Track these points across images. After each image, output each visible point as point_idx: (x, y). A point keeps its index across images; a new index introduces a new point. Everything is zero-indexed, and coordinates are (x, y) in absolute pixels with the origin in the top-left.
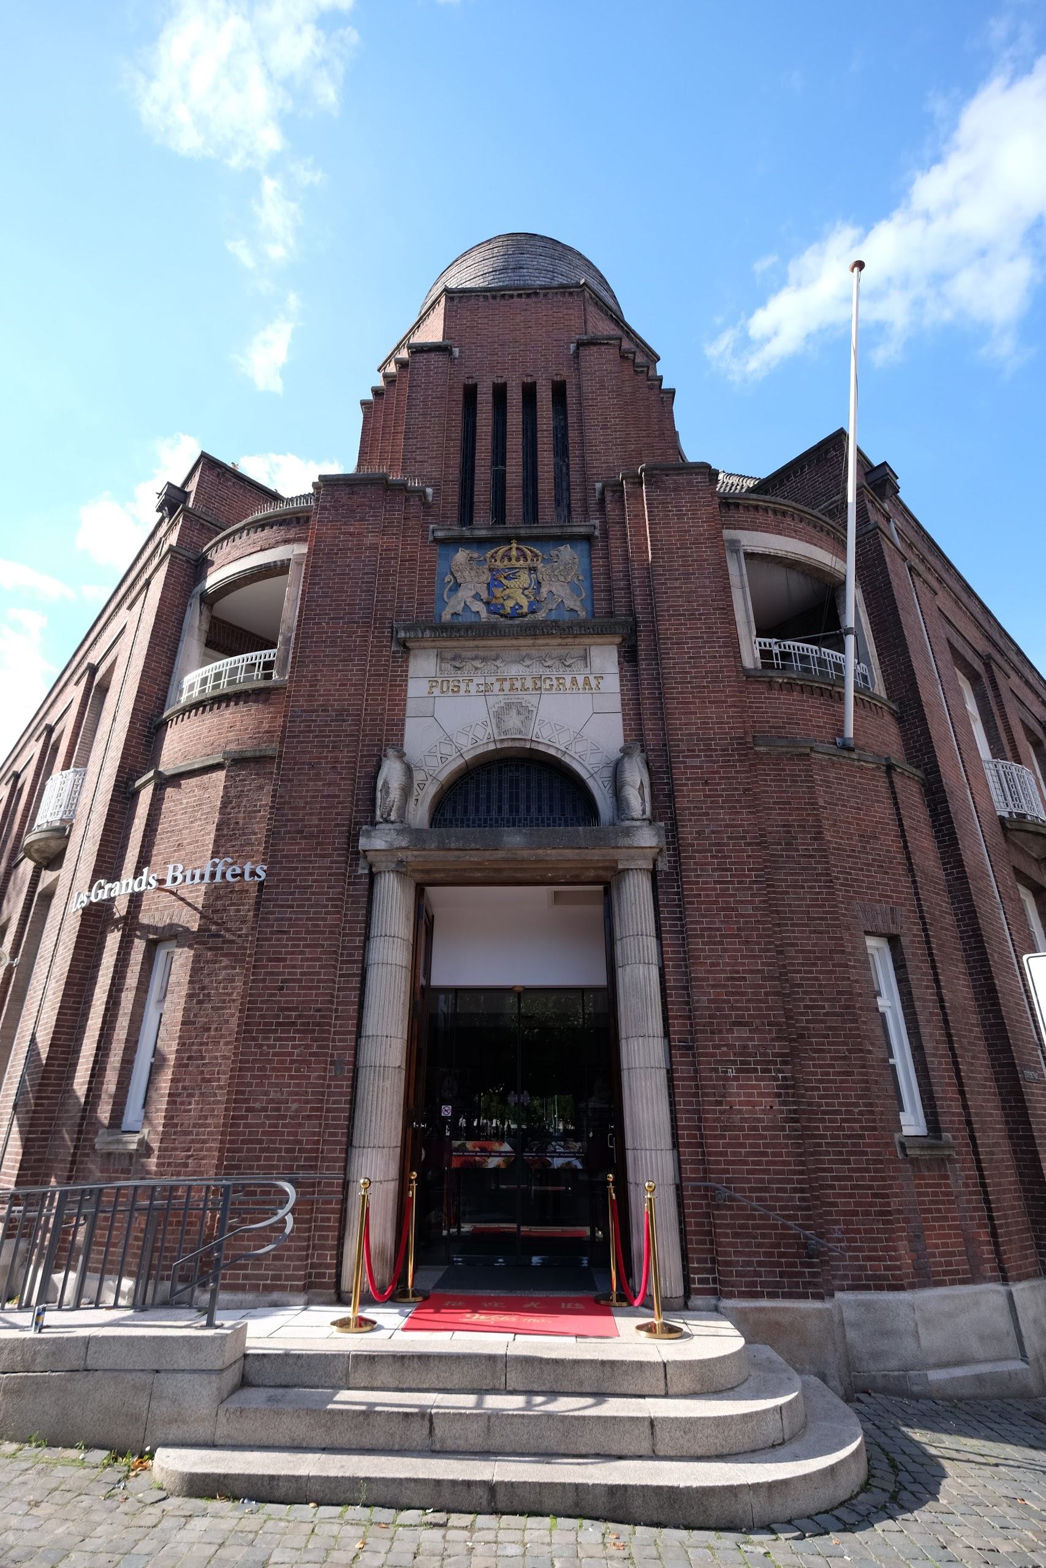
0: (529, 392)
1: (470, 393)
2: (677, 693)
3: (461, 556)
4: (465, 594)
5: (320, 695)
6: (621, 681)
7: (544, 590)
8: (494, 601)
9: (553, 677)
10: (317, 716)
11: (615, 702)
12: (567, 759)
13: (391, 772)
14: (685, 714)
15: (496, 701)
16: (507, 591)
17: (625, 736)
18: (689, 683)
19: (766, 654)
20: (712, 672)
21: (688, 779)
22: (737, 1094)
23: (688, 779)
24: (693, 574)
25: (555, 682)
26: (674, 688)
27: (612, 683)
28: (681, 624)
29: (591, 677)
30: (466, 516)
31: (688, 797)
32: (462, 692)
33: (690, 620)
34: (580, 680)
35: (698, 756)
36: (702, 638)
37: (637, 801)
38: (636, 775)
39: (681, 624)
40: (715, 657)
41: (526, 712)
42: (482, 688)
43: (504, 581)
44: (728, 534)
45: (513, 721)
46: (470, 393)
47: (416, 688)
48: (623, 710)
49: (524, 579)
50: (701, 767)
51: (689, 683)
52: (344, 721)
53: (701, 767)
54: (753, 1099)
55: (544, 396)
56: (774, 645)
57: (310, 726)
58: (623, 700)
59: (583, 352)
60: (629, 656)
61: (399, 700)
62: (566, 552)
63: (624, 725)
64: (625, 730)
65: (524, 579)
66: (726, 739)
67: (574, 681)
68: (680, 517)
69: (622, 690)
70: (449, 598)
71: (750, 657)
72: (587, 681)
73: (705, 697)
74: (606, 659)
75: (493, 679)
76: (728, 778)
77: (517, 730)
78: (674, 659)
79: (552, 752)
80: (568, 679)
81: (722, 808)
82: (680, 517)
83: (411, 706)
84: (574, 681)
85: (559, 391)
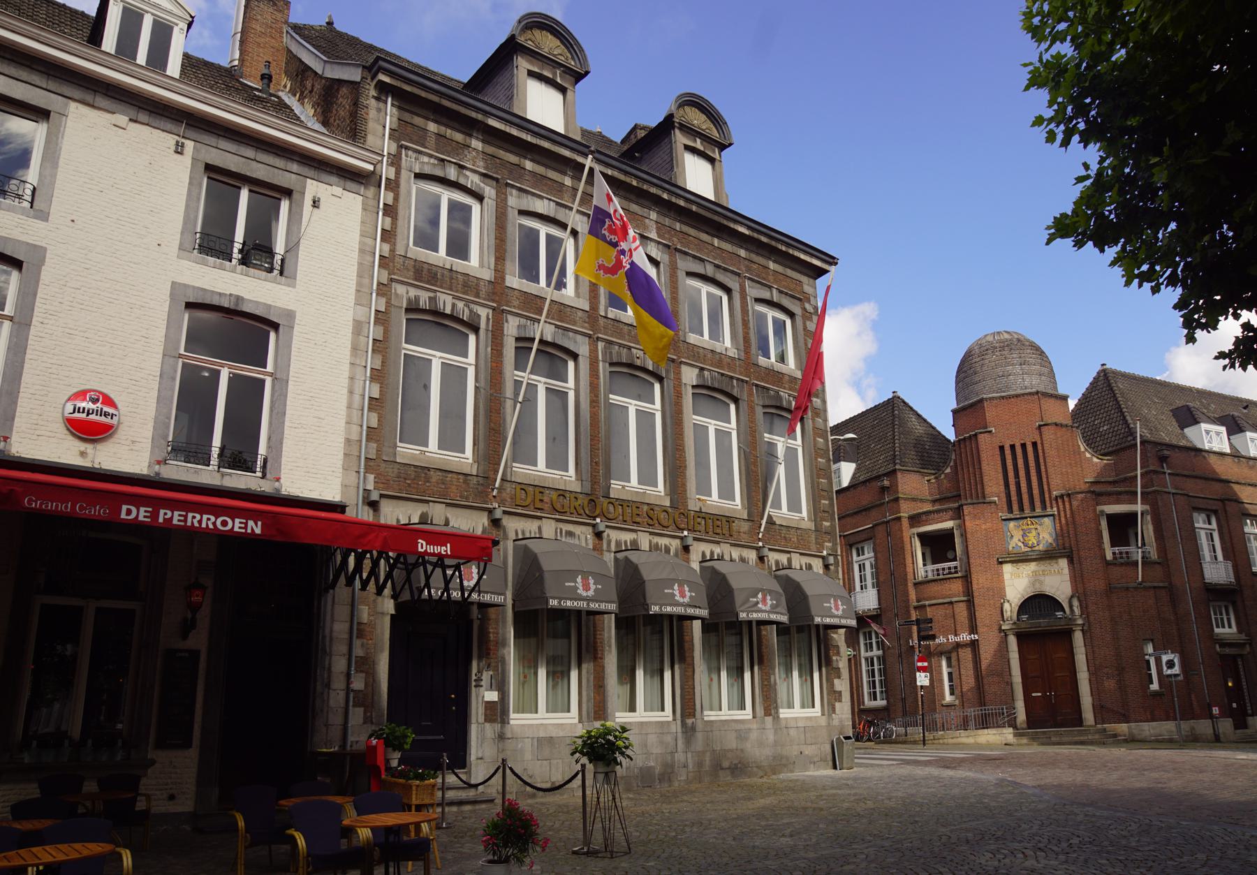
0: (1024, 446)
1: (1002, 448)
3: (1012, 524)
4: (1015, 539)
11: (1067, 578)
13: (1007, 606)
19: (1114, 553)
22: (1106, 684)
27: (1066, 571)
30: (1010, 510)
31: (1092, 608)
37: (1077, 611)
38: (1076, 603)
41: (1041, 583)
44: (1099, 508)
45: (1037, 585)
46: (1002, 448)
47: (1007, 576)
49: (1034, 533)
54: (1110, 684)
55: (1030, 449)
56: (1116, 549)
59: (1043, 429)
60: (1071, 562)
61: (1003, 581)
62: (1046, 519)
65: (1034, 533)
71: (1109, 556)
74: (1063, 563)
77: (1038, 589)
83: (1007, 583)
85: (1034, 444)
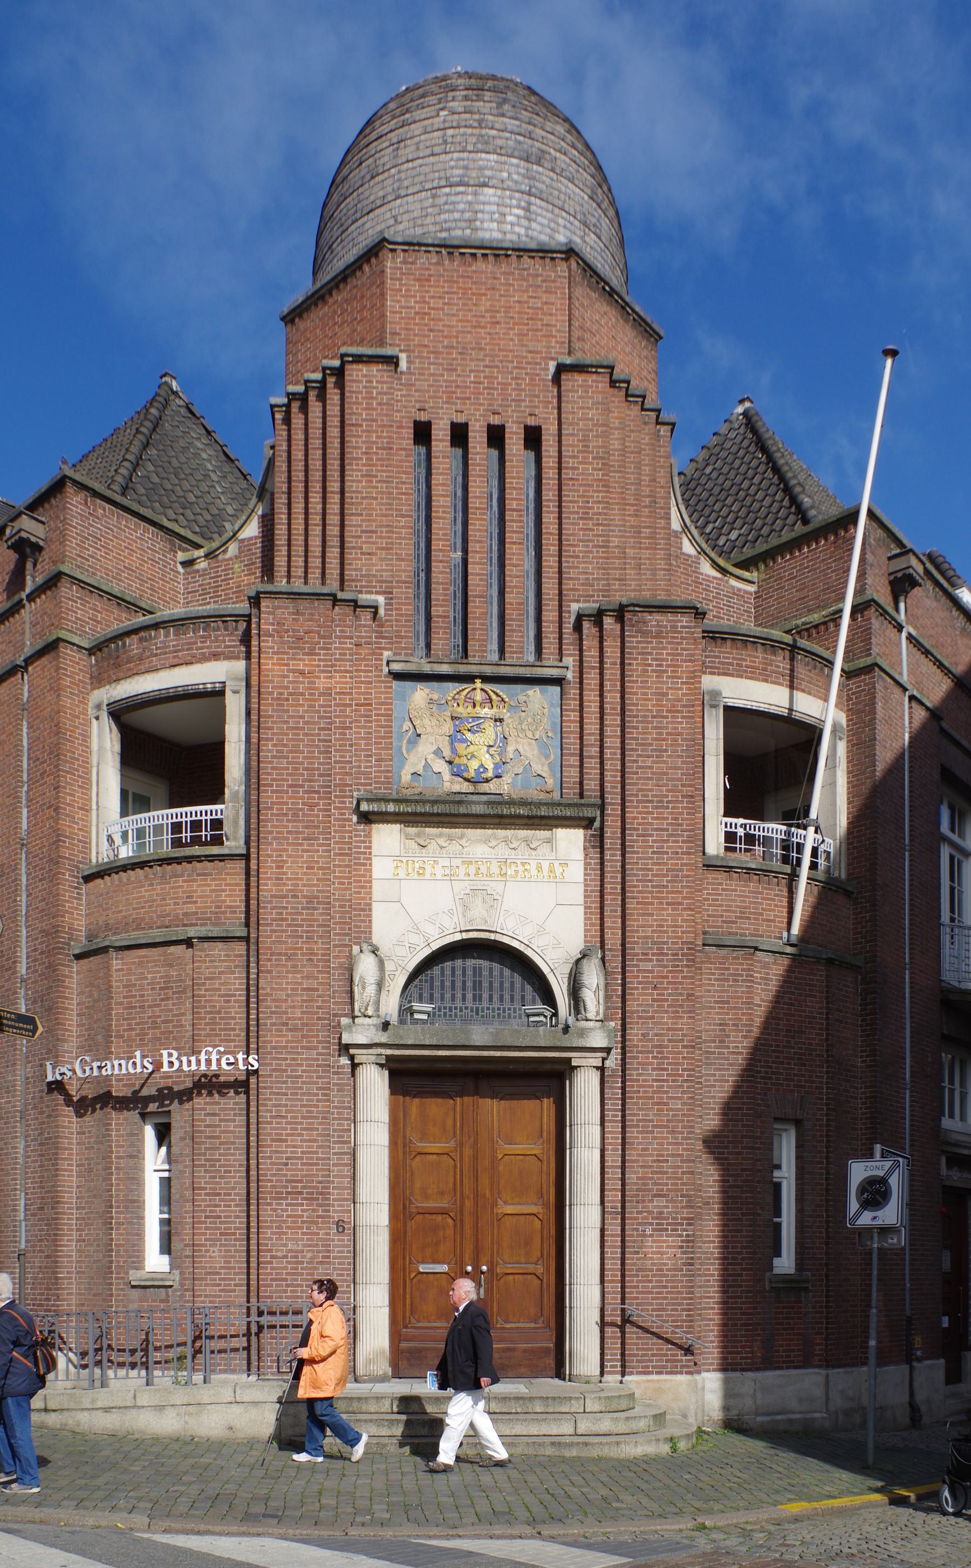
2: (639, 892)
3: (420, 694)
5: (288, 879)
6: (586, 869)
7: (510, 749)
8: (457, 761)
9: (519, 862)
10: (288, 902)
12: (529, 953)
14: (643, 915)
15: (462, 887)
16: (472, 748)
17: (586, 931)
18: (650, 881)
20: (673, 870)
21: (639, 983)
23: (639, 983)
24: (666, 751)
25: (521, 868)
26: (635, 886)
28: (648, 813)
29: (556, 864)
32: (427, 876)
33: (657, 807)
34: (545, 865)
35: (651, 960)
36: (667, 830)
39: (648, 813)
40: (677, 853)
41: (492, 900)
42: (448, 872)
43: (469, 736)
48: (586, 902)
50: (652, 971)
51: (650, 881)
52: (315, 909)
53: (652, 971)
57: (281, 914)
58: (586, 891)
63: (586, 919)
64: (586, 925)
66: (677, 943)
67: (539, 869)
68: (660, 673)
69: (585, 880)
70: (408, 751)
72: (552, 870)
73: (663, 898)
75: (457, 862)
76: (675, 983)
78: (637, 853)
79: (515, 944)
80: (534, 864)
81: (667, 1012)
82: (660, 673)
84: (539, 869)
